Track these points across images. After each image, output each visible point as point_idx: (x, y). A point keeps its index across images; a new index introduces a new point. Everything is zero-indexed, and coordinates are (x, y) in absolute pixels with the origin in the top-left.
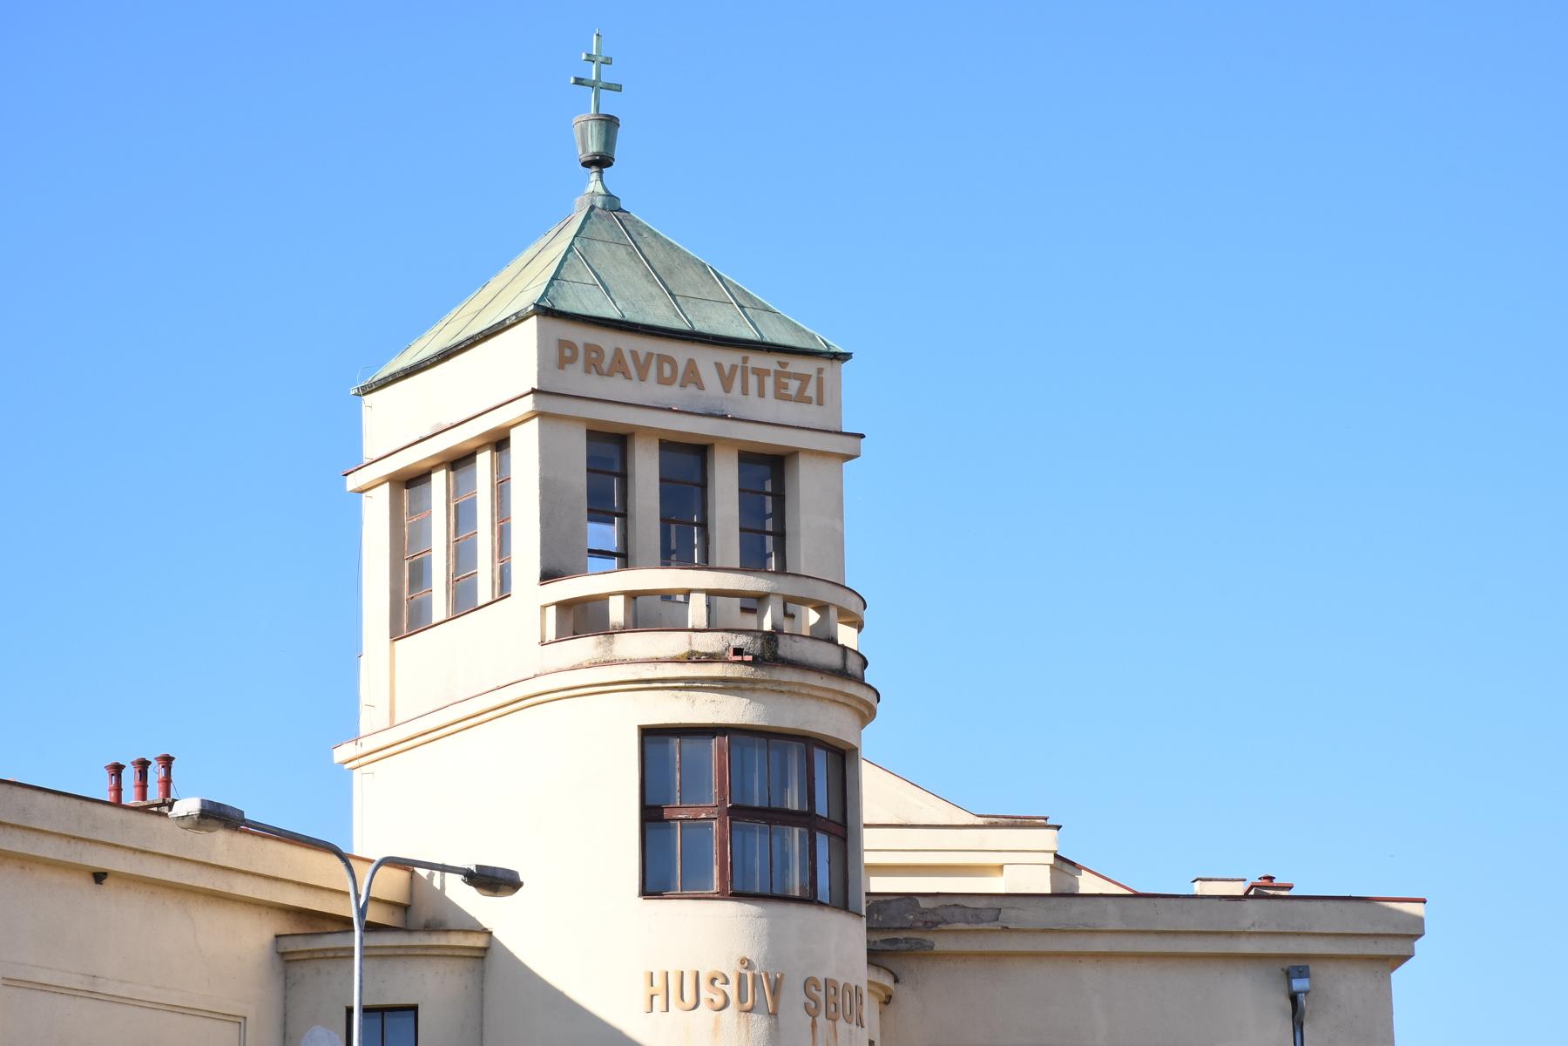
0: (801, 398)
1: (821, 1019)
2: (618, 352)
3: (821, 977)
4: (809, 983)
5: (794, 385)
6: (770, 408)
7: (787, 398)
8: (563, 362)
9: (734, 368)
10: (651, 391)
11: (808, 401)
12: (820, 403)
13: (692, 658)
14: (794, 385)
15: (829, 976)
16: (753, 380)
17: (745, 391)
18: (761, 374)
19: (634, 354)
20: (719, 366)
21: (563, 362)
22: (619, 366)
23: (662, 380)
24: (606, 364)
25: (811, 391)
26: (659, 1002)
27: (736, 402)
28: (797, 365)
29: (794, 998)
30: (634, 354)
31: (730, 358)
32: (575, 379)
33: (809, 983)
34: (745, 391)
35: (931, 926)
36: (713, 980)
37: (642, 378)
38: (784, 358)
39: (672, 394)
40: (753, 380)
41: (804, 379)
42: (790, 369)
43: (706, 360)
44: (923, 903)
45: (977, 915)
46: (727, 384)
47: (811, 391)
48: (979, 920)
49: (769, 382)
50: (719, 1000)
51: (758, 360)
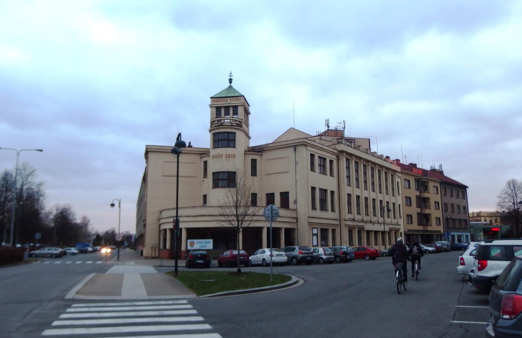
0: (239, 100)
1: (227, 158)
2: (219, 100)
6: (235, 102)
8: (213, 102)
10: (222, 103)
11: (239, 100)
13: (215, 126)
15: (229, 153)
16: (233, 100)
17: (232, 101)
21: (213, 102)
22: (219, 101)
23: (223, 102)
24: (218, 101)
28: (238, 98)
31: (230, 98)
32: (215, 103)
34: (232, 101)
37: (221, 101)
40: (233, 100)
41: (239, 99)
43: (228, 99)
46: (230, 101)
47: (240, 99)
51: (234, 98)
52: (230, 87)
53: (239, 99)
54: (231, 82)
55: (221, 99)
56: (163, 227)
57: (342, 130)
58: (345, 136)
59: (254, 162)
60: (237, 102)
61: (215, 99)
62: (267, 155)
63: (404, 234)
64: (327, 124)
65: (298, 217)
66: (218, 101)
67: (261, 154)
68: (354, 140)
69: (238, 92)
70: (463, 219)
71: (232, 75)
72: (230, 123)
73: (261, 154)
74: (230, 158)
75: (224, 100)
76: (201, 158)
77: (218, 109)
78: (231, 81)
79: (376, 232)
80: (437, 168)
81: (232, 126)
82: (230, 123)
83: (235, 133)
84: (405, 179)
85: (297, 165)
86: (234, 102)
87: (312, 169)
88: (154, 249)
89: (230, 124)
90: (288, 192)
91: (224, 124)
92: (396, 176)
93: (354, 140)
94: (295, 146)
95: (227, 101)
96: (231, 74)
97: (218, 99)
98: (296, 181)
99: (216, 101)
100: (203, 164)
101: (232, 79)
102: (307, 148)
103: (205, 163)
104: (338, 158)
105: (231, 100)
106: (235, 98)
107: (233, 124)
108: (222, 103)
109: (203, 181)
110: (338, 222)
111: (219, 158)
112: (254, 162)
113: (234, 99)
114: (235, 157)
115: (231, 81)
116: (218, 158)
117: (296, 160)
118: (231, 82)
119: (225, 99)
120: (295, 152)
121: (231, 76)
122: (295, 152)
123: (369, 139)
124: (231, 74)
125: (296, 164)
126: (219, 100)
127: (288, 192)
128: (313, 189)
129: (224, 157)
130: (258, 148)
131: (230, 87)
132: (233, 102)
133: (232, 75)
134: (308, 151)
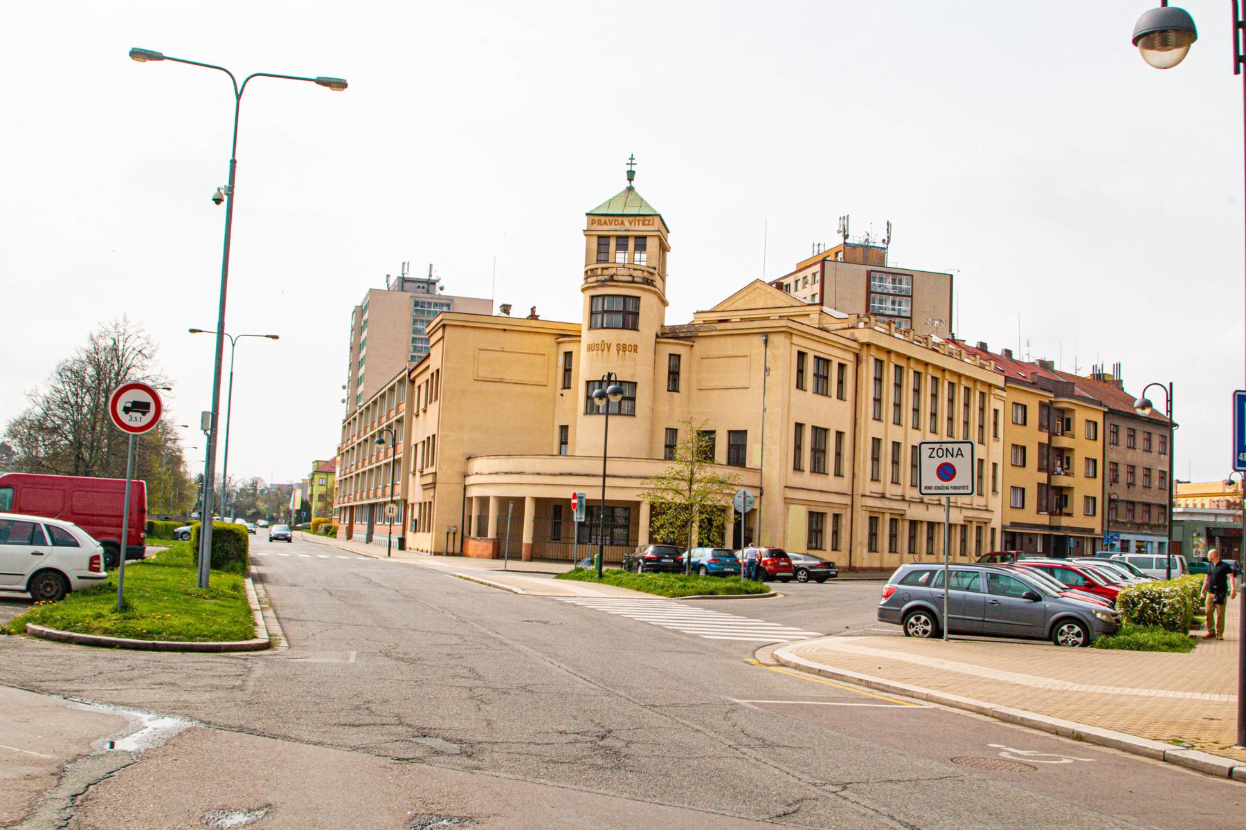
0: (649, 225)
1: (621, 352)
2: (605, 221)
5: (647, 222)
6: (641, 227)
10: (613, 227)
14: (647, 222)
21: (592, 224)
22: (605, 223)
23: (615, 225)
25: (651, 223)
27: (632, 228)
28: (647, 218)
31: (631, 219)
32: (595, 227)
37: (611, 224)
39: (618, 227)
41: (649, 221)
43: (626, 220)
46: (631, 224)
47: (651, 223)
49: (641, 223)
52: (630, 189)
53: (649, 221)
54: (630, 179)
55: (611, 218)
56: (473, 492)
57: (882, 248)
59: (675, 358)
61: (596, 218)
62: (701, 346)
63: (1002, 532)
64: (841, 229)
65: (764, 485)
67: (691, 343)
68: (912, 276)
69: (648, 206)
70: (1154, 504)
71: (634, 161)
72: (630, 275)
73: (691, 343)
74: (627, 353)
76: (558, 343)
77: (603, 240)
78: (631, 175)
79: (931, 525)
80: (1108, 370)
81: (633, 282)
82: (630, 275)
83: (639, 298)
84: (1014, 403)
85: (769, 375)
86: (639, 228)
87: (800, 385)
88: (451, 536)
89: (630, 279)
90: (745, 432)
91: (615, 278)
92: (992, 397)
93: (912, 276)
94: (766, 334)
95: (622, 223)
96: (632, 159)
97: (603, 219)
98: (765, 410)
99: (599, 223)
100: (561, 358)
101: (634, 172)
102: (791, 338)
103: (568, 355)
104: (858, 359)
106: (641, 218)
107: (636, 279)
108: (613, 227)
109: (562, 395)
110: (847, 500)
111: (603, 351)
112: (675, 358)
113: (639, 221)
114: (636, 351)
115: (631, 175)
116: (600, 351)
117: (767, 365)
118: (630, 179)
119: (620, 219)
121: (631, 164)
123: (951, 276)
124: (632, 159)
126: (605, 221)
127: (745, 432)
128: (799, 427)
129: (613, 349)
130: (685, 330)
131: (630, 189)
132: (637, 228)
133: (634, 161)
134: (793, 346)
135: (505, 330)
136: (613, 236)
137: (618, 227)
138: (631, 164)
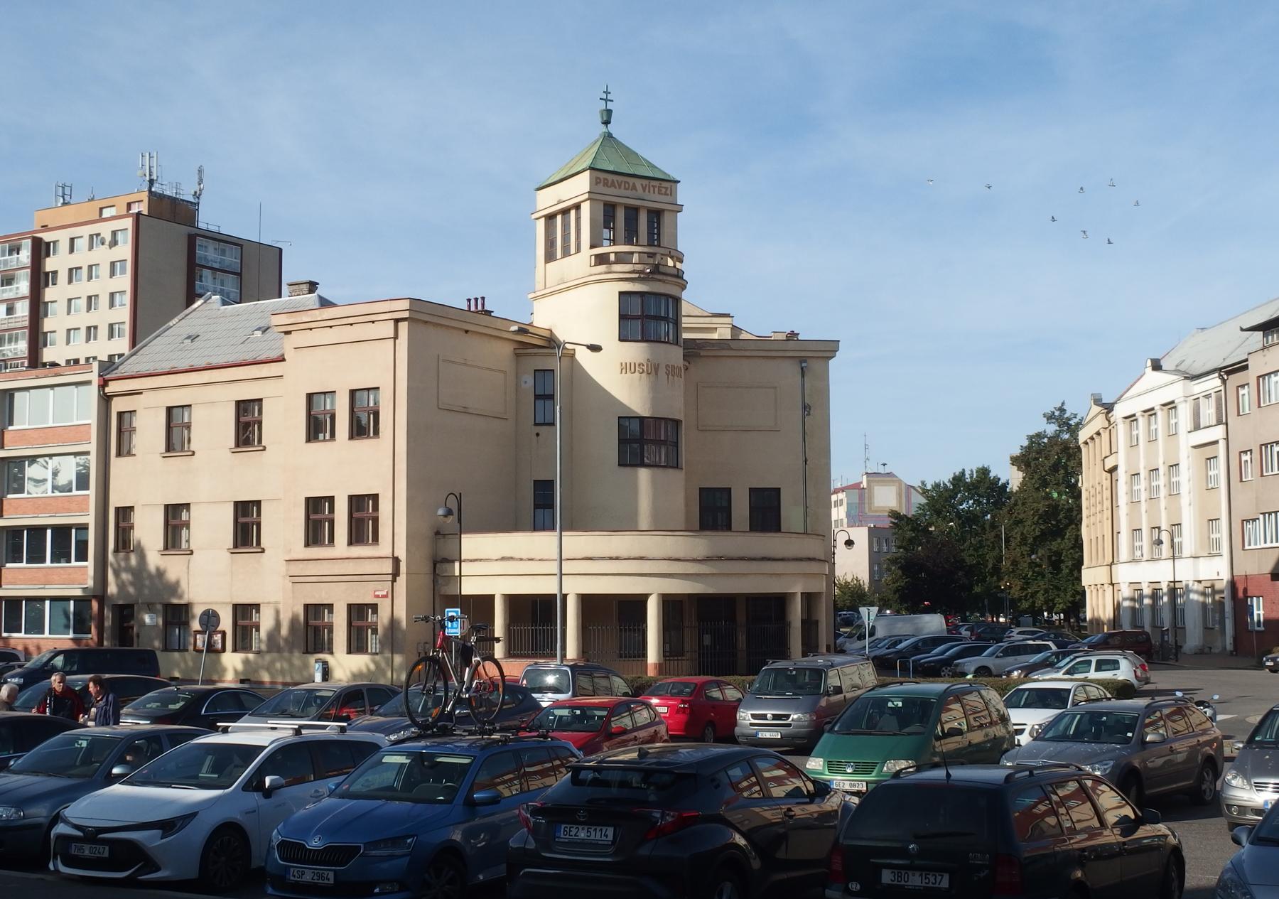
1: (670, 376)
3: (670, 364)
4: (667, 366)
7: (662, 194)
8: (597, 183)
9: (646, 185)
10: (622, 192)
11: (668, 195)
12: (671, 195)
14: (664, 190)
16: (652, 189)
17: (649, 192)
18: (654, 186)
19: (617, 181)
20: (642, 185)
21: (597, 183)
22: (613, 185)
23: (625, 189)
24: (609, 184)
25: (668, 192)
26: (624, 371)
29: (662, 371)
30: (617, 181)
31: (645, 182)
32: (601, 188)
33: (667, 366)
34: (649, 192)
35: (700, 349)
36: (639, 365)
37: (620, 188)
38: (660, 182)
39: (628, 193)
40: (652, 189)
41: (666, 188)
42: (663, 186)
43: (638, 182)
44: (697, 341)
45: (713, 345)
47: (668, 192)
48: (713, 346)
49: (656, 189)
50: (641, 371)
57: (191, 203)
58: (201, 225)
60: (663, 198)
66: (609, 184)
75: (628, 183)
85: (809, 414)
93: (241, 246)
95: (634, 188)
96: (607, 93)
97: (610, 177)
99: (606, 184)
105: (647, 191)
118: (607, 123)
119: (631, 180)
120: (803, 376)
122: (803, 376)
123: (281, 250)
124: (607, 93)
125: (806, 413)
135: (467, 332)
136: (620, 204)
137: (628, 193)
138: (606, 100)
